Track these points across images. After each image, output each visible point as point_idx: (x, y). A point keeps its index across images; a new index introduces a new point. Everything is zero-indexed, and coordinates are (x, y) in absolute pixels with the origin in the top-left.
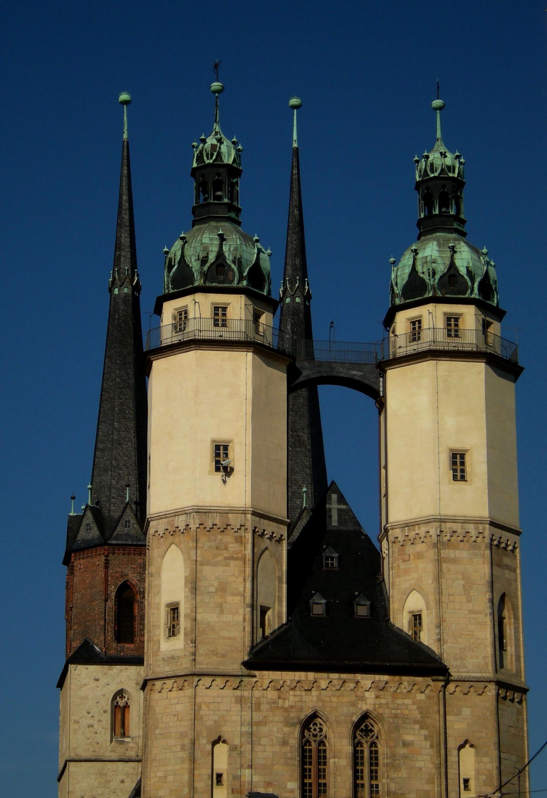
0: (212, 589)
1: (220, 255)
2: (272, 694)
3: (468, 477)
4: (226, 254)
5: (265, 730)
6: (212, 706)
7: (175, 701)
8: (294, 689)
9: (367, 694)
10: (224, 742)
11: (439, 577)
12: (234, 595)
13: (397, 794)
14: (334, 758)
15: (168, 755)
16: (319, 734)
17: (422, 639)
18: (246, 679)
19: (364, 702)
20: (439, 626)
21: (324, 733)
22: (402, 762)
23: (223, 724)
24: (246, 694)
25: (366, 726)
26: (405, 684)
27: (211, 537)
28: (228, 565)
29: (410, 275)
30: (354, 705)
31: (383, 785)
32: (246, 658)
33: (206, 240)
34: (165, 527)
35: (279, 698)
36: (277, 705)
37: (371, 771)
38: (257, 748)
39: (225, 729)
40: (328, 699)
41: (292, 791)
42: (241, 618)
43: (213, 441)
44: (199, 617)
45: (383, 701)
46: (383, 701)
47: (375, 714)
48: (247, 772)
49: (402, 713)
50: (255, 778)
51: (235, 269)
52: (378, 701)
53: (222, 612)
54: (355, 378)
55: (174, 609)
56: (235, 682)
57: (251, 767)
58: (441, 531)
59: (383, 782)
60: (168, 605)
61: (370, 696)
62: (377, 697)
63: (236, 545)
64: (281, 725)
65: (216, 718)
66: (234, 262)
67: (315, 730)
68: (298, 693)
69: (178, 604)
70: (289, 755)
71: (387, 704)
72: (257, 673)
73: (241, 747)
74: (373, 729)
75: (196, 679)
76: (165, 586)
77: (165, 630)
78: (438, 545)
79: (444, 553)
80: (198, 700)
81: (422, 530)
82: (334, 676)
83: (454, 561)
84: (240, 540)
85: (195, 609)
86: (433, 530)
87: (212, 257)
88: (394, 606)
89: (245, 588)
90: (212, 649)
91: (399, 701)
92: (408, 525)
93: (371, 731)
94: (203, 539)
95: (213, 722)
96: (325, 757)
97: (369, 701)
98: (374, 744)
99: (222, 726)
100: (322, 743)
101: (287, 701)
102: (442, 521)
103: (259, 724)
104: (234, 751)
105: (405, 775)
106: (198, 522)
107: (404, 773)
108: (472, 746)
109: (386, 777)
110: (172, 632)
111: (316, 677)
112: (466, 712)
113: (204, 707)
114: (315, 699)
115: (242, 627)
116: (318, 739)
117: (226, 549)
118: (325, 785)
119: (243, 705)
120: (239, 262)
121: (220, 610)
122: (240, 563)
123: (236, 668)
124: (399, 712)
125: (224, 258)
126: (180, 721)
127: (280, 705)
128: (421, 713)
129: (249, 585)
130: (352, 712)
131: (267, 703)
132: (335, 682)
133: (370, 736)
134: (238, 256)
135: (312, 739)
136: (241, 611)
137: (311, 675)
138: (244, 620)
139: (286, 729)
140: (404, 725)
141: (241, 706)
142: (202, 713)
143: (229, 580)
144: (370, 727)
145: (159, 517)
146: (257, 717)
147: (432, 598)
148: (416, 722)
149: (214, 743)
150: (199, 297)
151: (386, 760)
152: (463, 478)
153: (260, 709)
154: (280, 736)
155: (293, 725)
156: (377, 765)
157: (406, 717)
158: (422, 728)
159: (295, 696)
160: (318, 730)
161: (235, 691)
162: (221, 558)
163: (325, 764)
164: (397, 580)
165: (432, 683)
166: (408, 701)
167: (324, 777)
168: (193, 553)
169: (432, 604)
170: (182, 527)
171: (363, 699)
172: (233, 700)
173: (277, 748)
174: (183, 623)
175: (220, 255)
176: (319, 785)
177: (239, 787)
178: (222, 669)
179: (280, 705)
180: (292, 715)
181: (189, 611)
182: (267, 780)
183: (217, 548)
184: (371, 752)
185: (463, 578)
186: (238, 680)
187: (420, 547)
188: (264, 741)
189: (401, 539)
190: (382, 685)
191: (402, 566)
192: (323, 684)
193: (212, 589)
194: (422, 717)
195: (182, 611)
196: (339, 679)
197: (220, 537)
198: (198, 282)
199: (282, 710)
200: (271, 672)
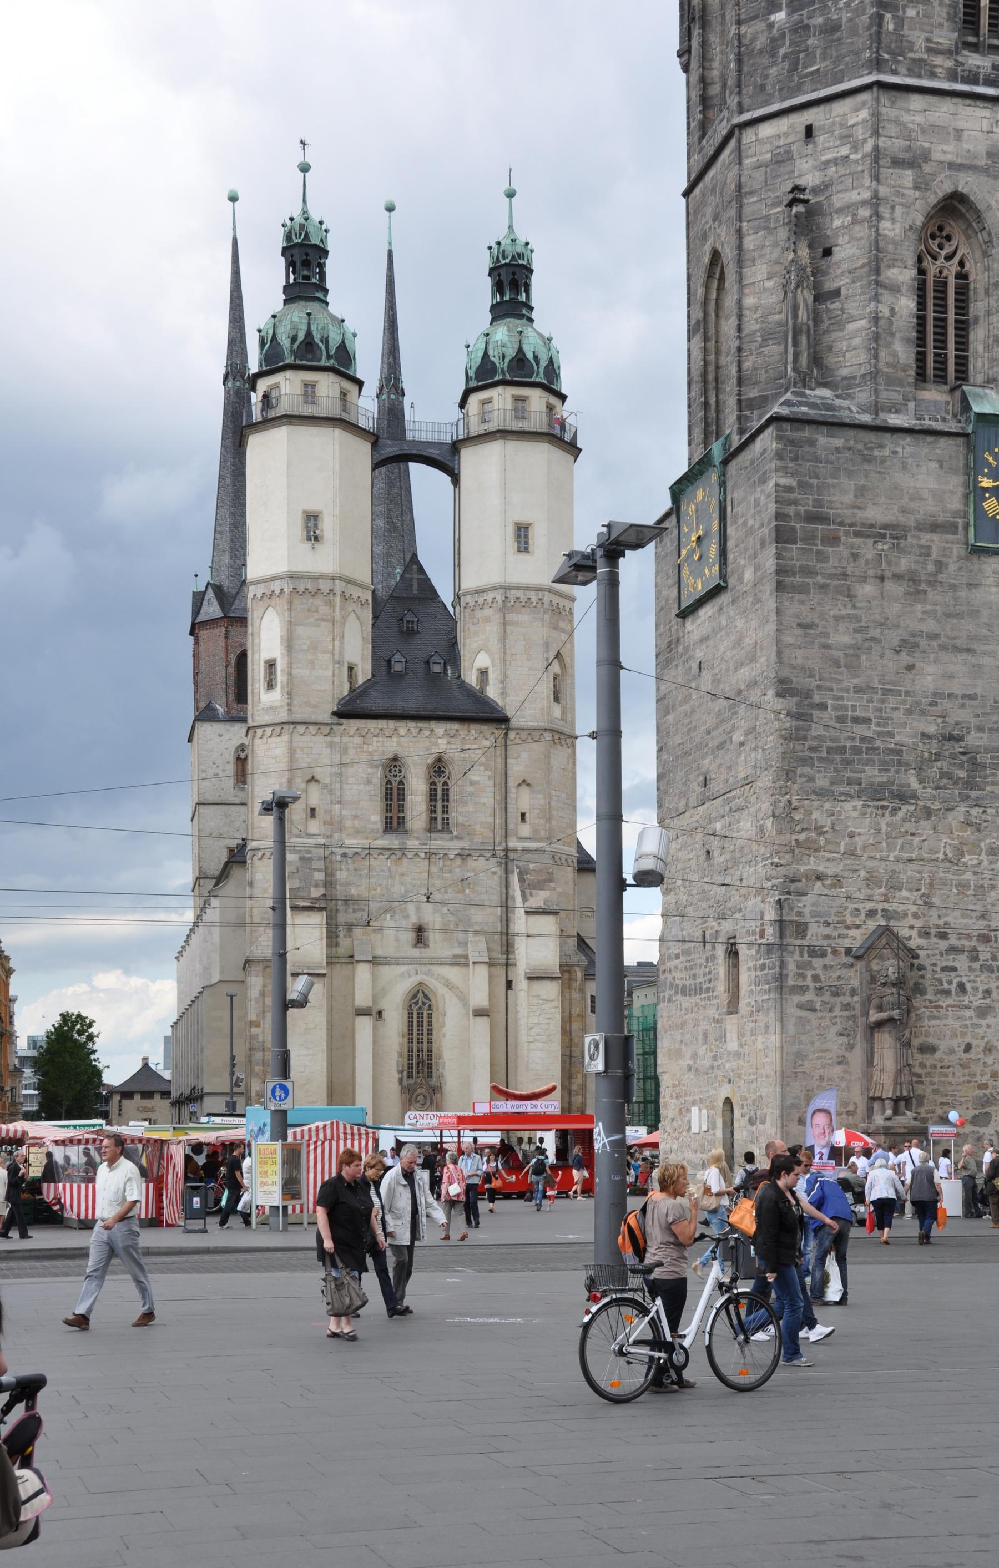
0: (305, 647)
1: (309, 334)
2: (358, 740)
3: (530, 549)
4: (314, 333)
5: (351, 770)
6: (305, 750)
7: (274, 746)
8: (375, 736)
9: (439, 741)
10: (317, 781)
11: (504, 637)
12: (324, 652)
18: (335, 727)
20: (503, 682)
21: (403, 774)
24: (337, 739)
25: (439, 768)
26: (473, 732)
28: (318, 626)
29: (483, 359)
32: (335, 709)
33: (296, 319)
37: (443, 806)
38: (345, 787)
41: (375, 823)
42: (330, 673)
43: (305, 512)
44: (294, 672)
46: (453, 746)
47: (446, 757)
48: (337, 807)
50: (344, 812)
51: (323, 348)
52: (449, 746)
54: (433, 456)
55: (271, 665)
56: (326, 730)
57: (339, 802)
58: (506, 598)
59: (453, 815)
60: (266, 662)
62: (449, 743)
63: (326, 608)
65: (309, 760)
66: (322, 341)
68: (380, 739)
69: (275, 660)
70: (373, 793)
72: (344, 721)
75: (292, 726)
76: (263, 645)
78: (505, 608)
79: (509, 617)
80: (294, 744)
81: (490, 596)
82: (412, 724)
83: (517, 624)
84: (330, 604)
85: (290, 664)
86: (499, 597)
87: (301, 336)
88: (464, 664)
89: (334, 646)
92: (477, 592)
93: (444, 772)
94: (296, 602)
96: (403, 794)
97: (441, 747)
98: (445, 784)
100: (401, 783)
102: (508, 588)
106: (292, 587)
107: (470, 808)
108: (528, 785)
110: (270, 685)
112: (524, 756)
113: (298, 750)
114: (395, 744)
116: (398, 779)
117: (317, 611)
118: (403, 818)
120: (326, 341)
122: (329, 624)
123: (325, 716)
125: (313, 338)
129: (337, 643)
132: (412, 730)
134: (325, 336)
135: (393, 779)
136: (331, 667)
138: (334, 675)
139: (370, 770)
142: (297, 756)
145: (257, 582)
146: (346, 759)
147: (497, 656)
149: (309, 781)
150: (289, 374)
152: (526, 550)
155: (377, 767)
156: (448, 801)
158: (486, 770)
162: (312, 620)
163: (403, 800)
164: (468, 641)
165: (496, 731)
167: (403, 811)
168: (287, 614)
169: (497, 662)
170: (277, 591)
171: (436, 744)
173: (362, 787)
174: (280, 678)
175: (309, 334)
176: (399, 818)
178: (314, 718)
181: (285, 666)
183: (309, 610)
184: (443, 790)
185: (525, 640)
186: (329, 728)
187: (488, 612)
188: (351, 780)
189: (471, 604)
190: (452, 733)
191: (472, 628)
192: (402, 731)
193: (305, 647)
195: (279, 667)
196: (416, 727)
197: (311, 600)
198: (289, 360)
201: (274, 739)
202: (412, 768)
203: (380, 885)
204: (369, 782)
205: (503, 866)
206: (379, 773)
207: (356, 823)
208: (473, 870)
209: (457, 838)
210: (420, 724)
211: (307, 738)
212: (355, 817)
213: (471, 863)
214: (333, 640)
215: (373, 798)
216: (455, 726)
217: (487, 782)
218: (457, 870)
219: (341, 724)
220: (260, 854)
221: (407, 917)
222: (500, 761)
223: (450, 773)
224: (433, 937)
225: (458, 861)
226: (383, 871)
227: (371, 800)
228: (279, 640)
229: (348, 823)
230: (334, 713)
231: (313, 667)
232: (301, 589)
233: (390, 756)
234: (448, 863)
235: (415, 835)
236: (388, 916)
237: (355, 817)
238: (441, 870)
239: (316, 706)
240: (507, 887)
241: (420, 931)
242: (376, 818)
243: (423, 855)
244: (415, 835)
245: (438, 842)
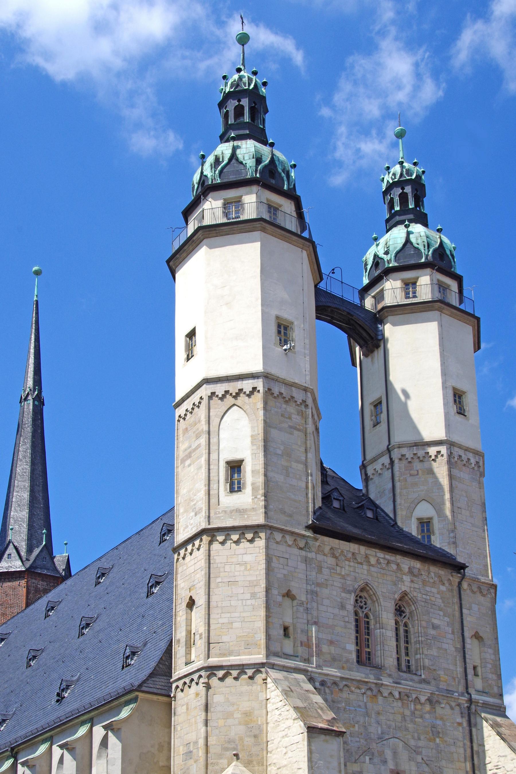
0: (279, 452)
2: (331, 561)
5: (325, 592)
9: (404, 577)
13: (430, 669)
14: (382, 629)
15: (233, 603)
16: (364, 606)
17: (434, 542)
19: (403, 584)
22: (432, 641)
23: (291, 579)
24: (310, 555)
27: (277, 404)
28: (291, 434)
30: (395, 584)
31: (416, 660)
34: (225, 388)
35: (337, 565)
36: (335, 572)
38: (321, 608)
39: (293, 584)
40: (375, 575)
41: (350, 652)
42: (303, 485)
45: (416, 586)
46: (416, 586)
47: (411, 595)
49: (430, 599)
53: (288, 476)
60: (228, 463)
61: (407, 579)
62: (412, 581)
64: (339, 590)
65: (285, 572)
67: (361, 602)
68: (352, 564)
70: (347, 619)
71: (419, 589)
73: (307, 604)
74: (405, 610)
77: (225, 485)
82: (380, 554)
90: (280, 507)
91: (428, 589)
93: (404, 612)
95: (282, 576)
98: (406, 625)
99: (290, 580)
101: (343, 569)
103: (318, 585)
104: (301, 606)
105: (435, 654)
109: (421, 653)
111: (367, 553)
114: (366, 572)
115: (305, 493)
119: (308, 565)
121: (286, 473)
124: (428, 597)
126: (250, 570)
127: (338, 572)
128: (443, 602)
130: (394, 590)
131: (327, 568)
133: (403, 617)
136: (304, 478)
137: (363, 549)
139: (343, 595)
140: (432, 610)
141: (306, 566)
143: (293, 447)
144: (403, 609)
146: (321, 579)
148: (440, 609)
151: (420, 638)
153: (322, 572)
154: (339, 600)
155: (349, 592)
157: (433, 603)
158: (444, 615)
159: (350, 566)
160: (364, 603)
161: (300, 551)
162: (285, 425)
166: (434, 590)
172: (299, 559)
173: (336, 611)
177: (306, 640)
179: (338, 572)
180: (348, 583)
182: (330, 639)
183: (282, 415)
188: (326, 602)
193: (279, 452)
194: (444, 606)
196: (384, 558)
199: (340, 577)
200: (331, 539)
201: (245, 544)
202: (381, 600)
203: (358, 722)
204: (343, 607)
205: (467, 718)
206: (352, 598)
207: (332, 649)
208: (442, 719)
209: (425, 681)
210: (387, 557)
211: (282, 548)
212: (331, 643)
214: (306, 451)
215: (347, 624)
216: (417, 565)
217: (447, 628)
218: (427, 716)
219: (316, 539)
220: (221, 673)
223: (411, 613)
225: (428, 707)
226: (359, 706)
227: (345, 627)
228: (249, 440)
230: (308, 527)
231: (288, 476)
232: (276, 390)
233: (361, 583)
234: (419, 707)
235: (388, 671)
237: (331, 643)
238: (413, 713)
239: (290, 516)
242: (352, 647)
243: (397, 695)
244: (388, 671)
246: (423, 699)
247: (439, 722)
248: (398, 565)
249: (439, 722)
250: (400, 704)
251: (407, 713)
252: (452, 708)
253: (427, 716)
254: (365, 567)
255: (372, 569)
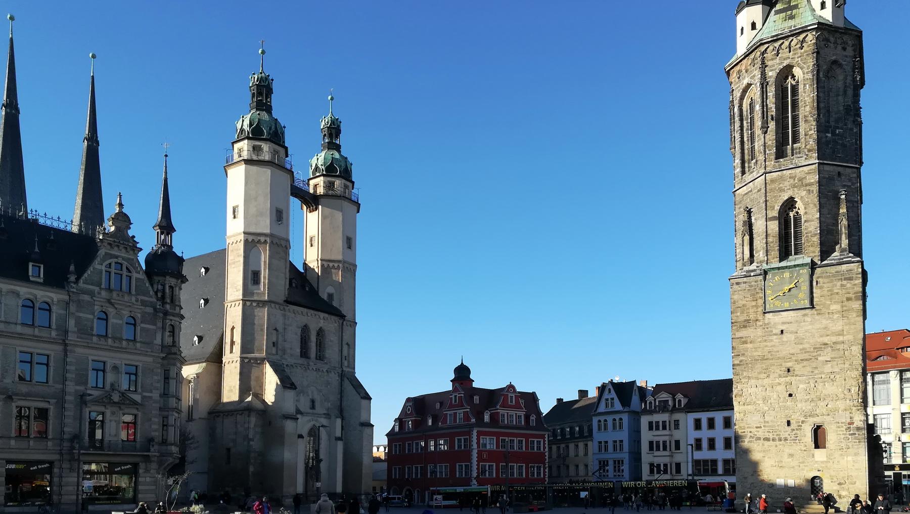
9: (321, 321)
56: (282, 308)
61: (322, 321)
62: (324, 322)
82: (312, 312)
91: (330, 325)
123: (282, 302)
132: (313, 314)
148: (334, 334)
155: (299, 328)
171: (320, 322)
204: (296, 334)
209: (326, 363)
213: (330, 375)
216: (326, 315)
219: (288, 306)
221: (308, 396)
222: (341, 333)
224: (317, 405)
225: (326, 374)
229: (289, 351)
236: (302, 394)
240: (341, 386)
241: (313, 402)
242: (299, 350)
245: (320, 364)
246: (325, 370)
247: (330, 380)
248: (319, 316)
249: (330, 380)
250: (315, 372)
251: (318, 376)
252: (335, 374)
253: (325, 377)
254: (306, 317)
255: (309, 318)
